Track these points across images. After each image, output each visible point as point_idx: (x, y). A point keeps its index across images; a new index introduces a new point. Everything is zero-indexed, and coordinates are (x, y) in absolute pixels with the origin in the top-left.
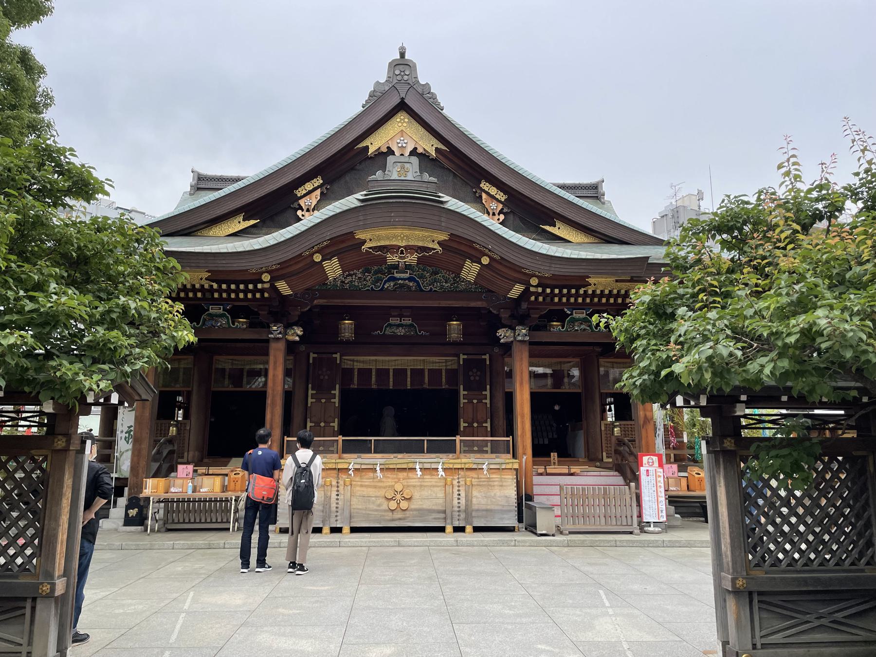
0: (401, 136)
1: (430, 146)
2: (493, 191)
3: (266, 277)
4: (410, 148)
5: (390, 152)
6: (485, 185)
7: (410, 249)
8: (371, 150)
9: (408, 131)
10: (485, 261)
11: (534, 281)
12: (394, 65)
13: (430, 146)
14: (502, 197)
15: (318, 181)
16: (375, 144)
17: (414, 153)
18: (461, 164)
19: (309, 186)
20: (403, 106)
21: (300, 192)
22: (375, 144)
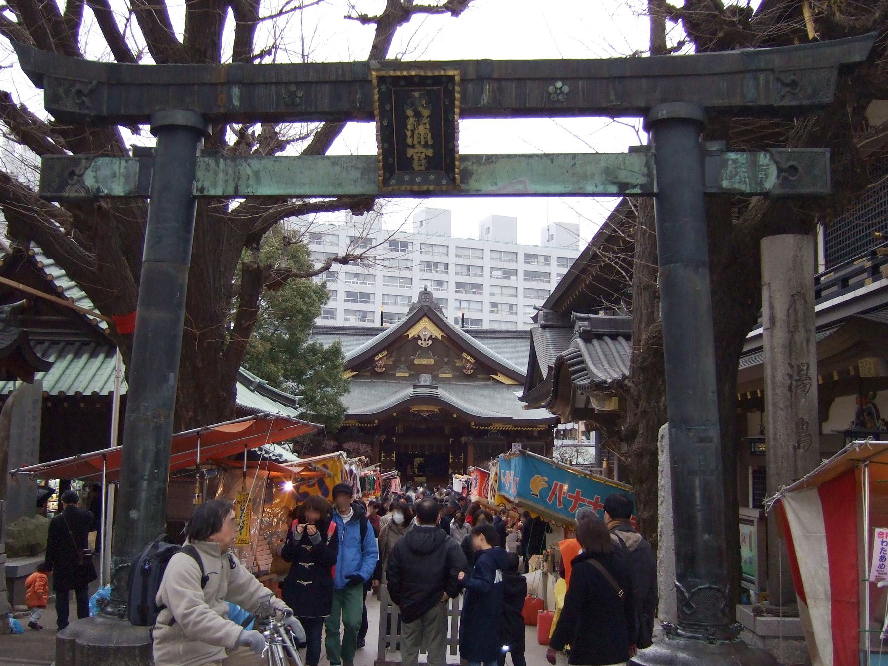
0: (425, 329)
1: (438, 334)
2: (468, 358)
3: (377, 421)
4: (428, 336)
5: (419, 338)
6: (464, 355)
7: (427, 411)
8: (411, 336)
9: (428, 327)
10: (455, 416)
11: (473, 424)
12: (421, 294)
13: (438, 334)
14: (472, 361)
15: (385, 353)
16: (412, 333)
17: (430, 338)
18: (451, 345)
19: (381, 356)
20: (425, 315)
21: (377, 358)
22: (412, 333)
